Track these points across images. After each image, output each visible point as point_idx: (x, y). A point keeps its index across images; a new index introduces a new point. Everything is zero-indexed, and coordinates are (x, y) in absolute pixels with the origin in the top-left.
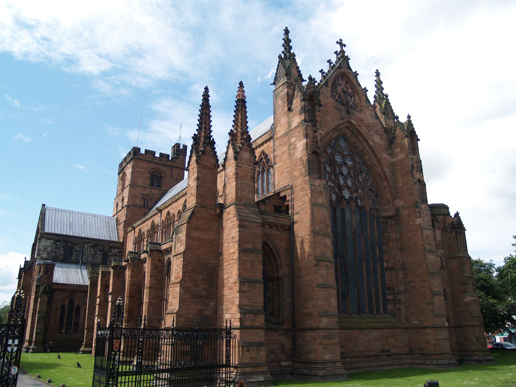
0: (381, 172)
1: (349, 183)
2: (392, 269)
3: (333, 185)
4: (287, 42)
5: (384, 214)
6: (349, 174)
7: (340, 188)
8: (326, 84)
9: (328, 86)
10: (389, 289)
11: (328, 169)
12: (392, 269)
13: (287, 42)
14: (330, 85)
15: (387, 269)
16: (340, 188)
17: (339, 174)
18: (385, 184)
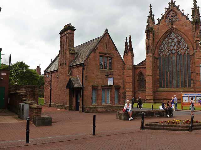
0: (188, 40)
1: (175, 48)
2: (193, 73)
3: (168, 50)
4: (151, 10)
5: (191, 54)
6: (175, 45)
7: (171, 51)
8: (162, 18)
9: (163, 19)
10: (192, 79)
11: (166, 46)
12: (193, 73)
13: (151, 10)
14: (164, 18)
15: (191, 73)
16: (171, 51)
18: (190, 44)
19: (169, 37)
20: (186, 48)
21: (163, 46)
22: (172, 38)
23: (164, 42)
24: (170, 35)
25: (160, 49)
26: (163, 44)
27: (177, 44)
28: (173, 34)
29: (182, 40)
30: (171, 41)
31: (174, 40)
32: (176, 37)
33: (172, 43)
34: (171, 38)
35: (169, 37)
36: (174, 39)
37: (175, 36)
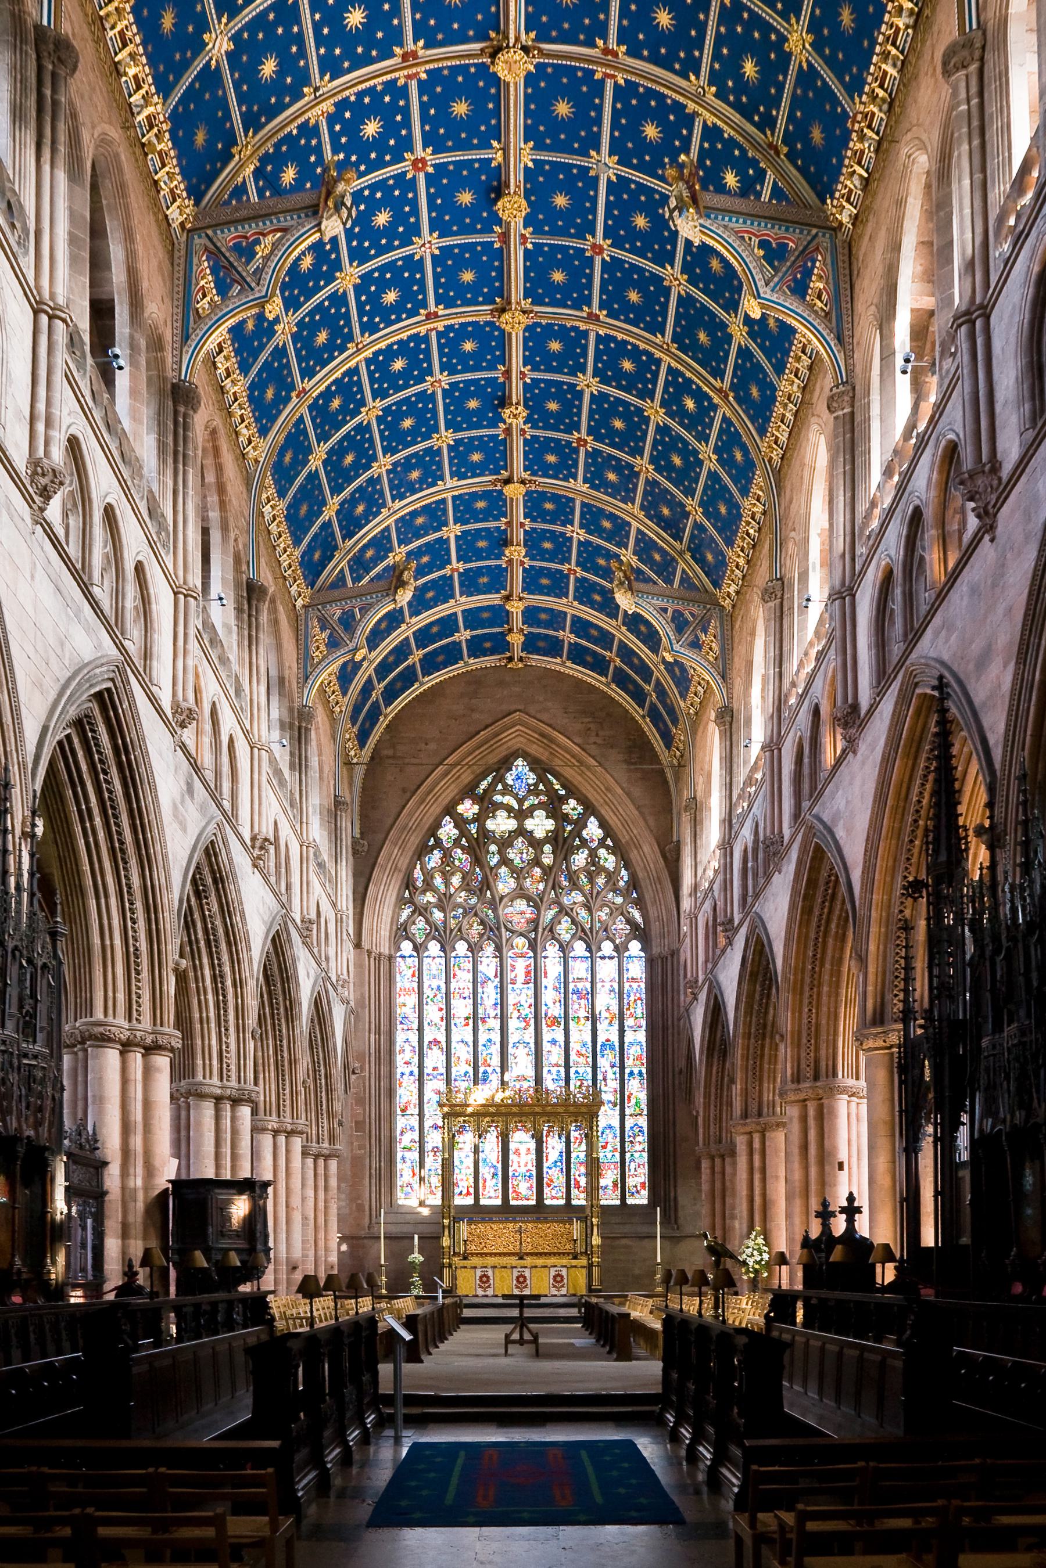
6: (537, 862)
17: (499, 865)
19: (491, 790)
20: (619, 900)
21: (434, 859)
22: (516, 807)
23: (448, 831)
24: (501, 779)
25: (408, 883)
26: (438, 843)
27: (547, 860)
28: (520, 773)
29: (593, 830)
30: (501, 824)
31: (529, 824)
32: (543, 798)
33: (505, 843)
34: (508, 800)
35: (491, 790)
36: (529, 813)
37: (533, 791)
